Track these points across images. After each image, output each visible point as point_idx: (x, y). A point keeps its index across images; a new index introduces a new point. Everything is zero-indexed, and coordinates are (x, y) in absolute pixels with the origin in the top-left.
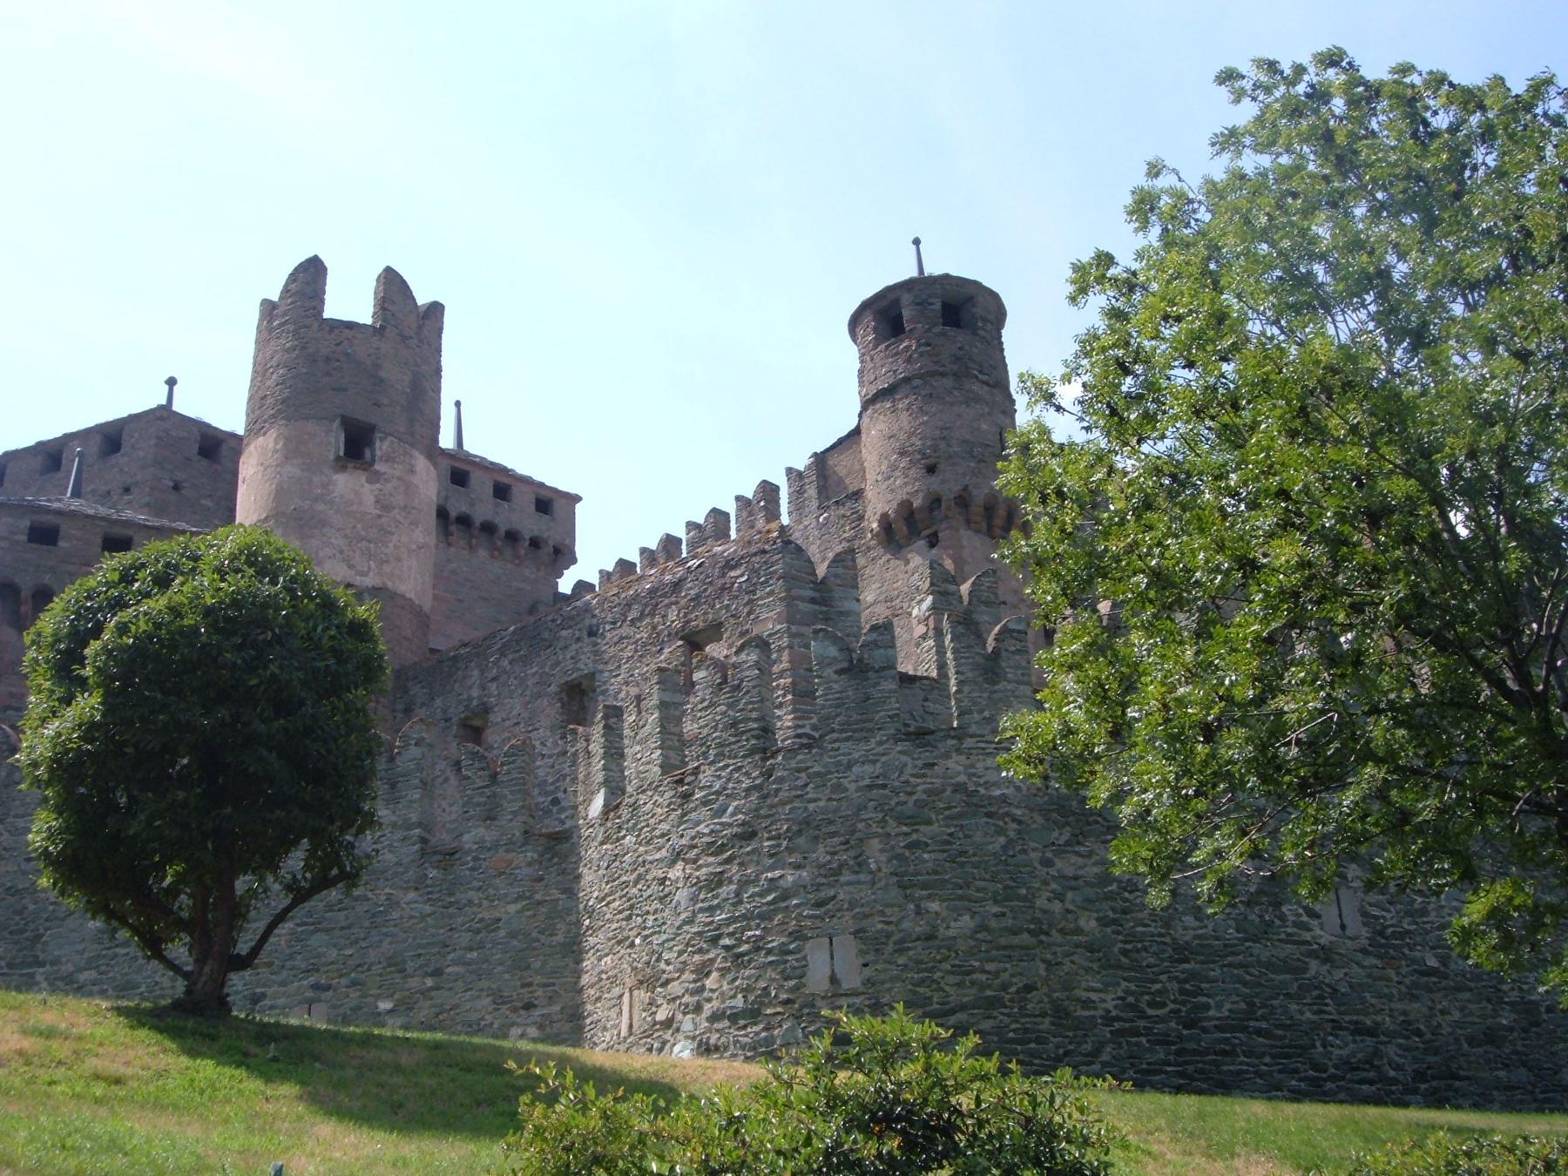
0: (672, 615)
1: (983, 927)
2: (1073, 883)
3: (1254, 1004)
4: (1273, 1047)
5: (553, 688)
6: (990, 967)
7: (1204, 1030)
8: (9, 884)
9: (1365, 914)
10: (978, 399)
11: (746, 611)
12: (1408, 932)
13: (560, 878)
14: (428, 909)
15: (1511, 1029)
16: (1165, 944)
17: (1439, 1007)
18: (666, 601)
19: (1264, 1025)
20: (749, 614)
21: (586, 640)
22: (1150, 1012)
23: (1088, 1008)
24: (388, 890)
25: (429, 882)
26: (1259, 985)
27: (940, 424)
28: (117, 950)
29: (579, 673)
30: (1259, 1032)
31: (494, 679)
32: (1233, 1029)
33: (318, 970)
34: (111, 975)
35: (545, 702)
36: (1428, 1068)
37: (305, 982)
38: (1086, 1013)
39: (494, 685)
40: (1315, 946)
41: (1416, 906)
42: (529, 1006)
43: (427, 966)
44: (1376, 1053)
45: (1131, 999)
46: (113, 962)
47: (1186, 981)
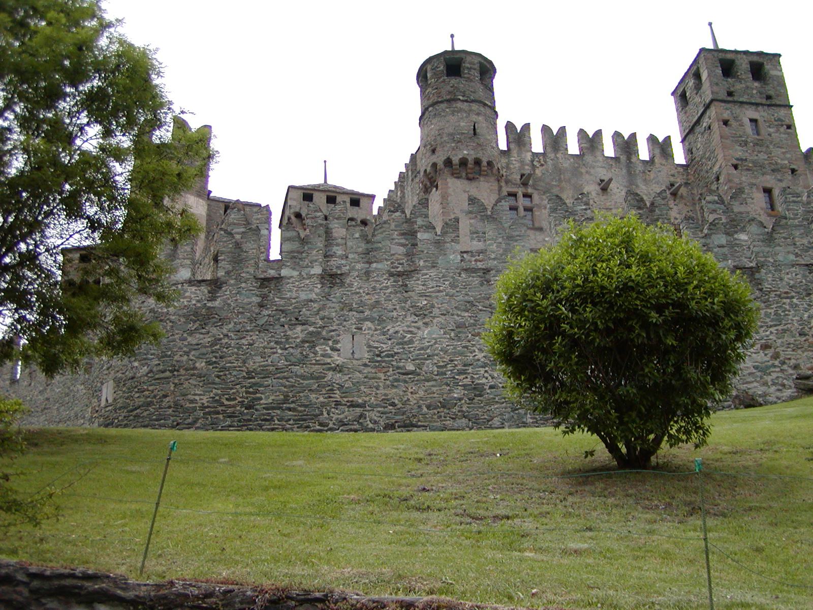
1: (151, 371)
2: (196, 347)
3: (288, 396)
4: (296, 415)
6: (150, 388)
7: (257, 410)
9: (369, 346)
10: (460, 110)
12: (398, 353)
15: (460, 399)
16: (242, 371)
17: (410, 390)
19: (292, 406)
22: (226, 403)
23: (193, 403)
26: (293, 386)
27: (438, 128)
30: (290, 409)
32: (273, 408)
36: (396, 422)
38: (191, 405)
40: (333, 365)
41: (406, 339)
44: (361, 416)
45: (217, 398)
47: (250, 387)
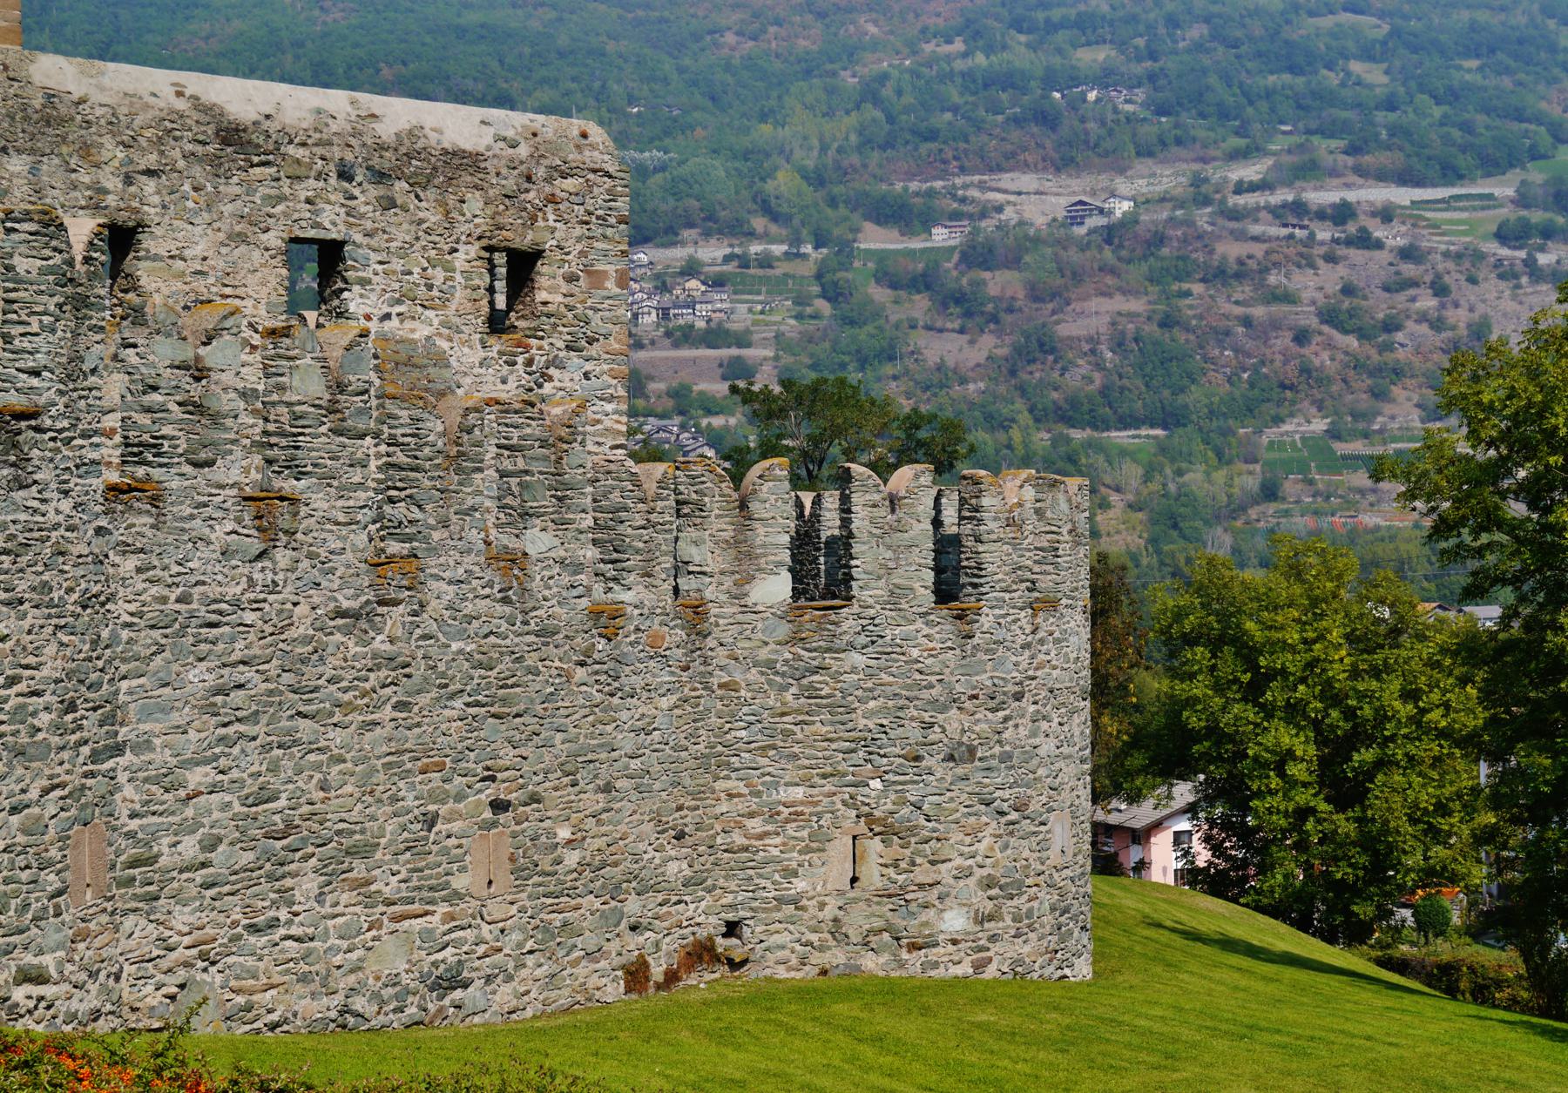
0: (475, 203)
5: (274, 239)
8: (83, 586)
11: (579, 247)
13: (702, 668)
14: (598, 697)
18: (469, 179)
20: (582, 254)
21: (333, 181)
24: (557, 664)
25: (596, 656)
28: (241, 728)
29: (321, 235)
31: (150, 173)
33: (493, 779)
34: (235, 774)
35: (256, 254)
37: (483, 796)
39: (150, 185)
42: (680, 836)
43: (596, 776)
46: (236, 750)
